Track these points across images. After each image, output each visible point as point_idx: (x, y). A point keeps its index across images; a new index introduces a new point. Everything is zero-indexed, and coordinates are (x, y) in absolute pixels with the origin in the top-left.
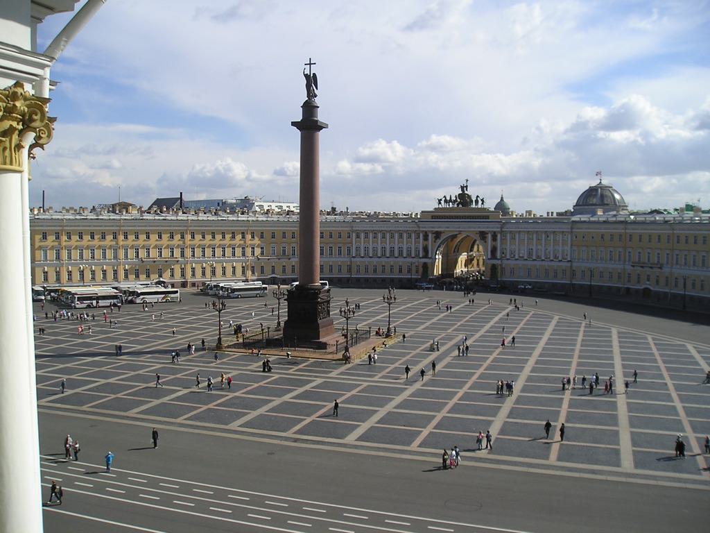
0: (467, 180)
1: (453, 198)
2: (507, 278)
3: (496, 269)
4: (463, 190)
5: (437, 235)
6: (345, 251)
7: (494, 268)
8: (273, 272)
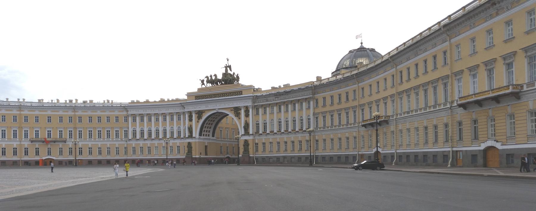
1: (214, 78)
2: (260, 154)
4: (226, 70)
5: (200, 114)
6: (122, 134)
7: (246, 143)
8: (49, 153)
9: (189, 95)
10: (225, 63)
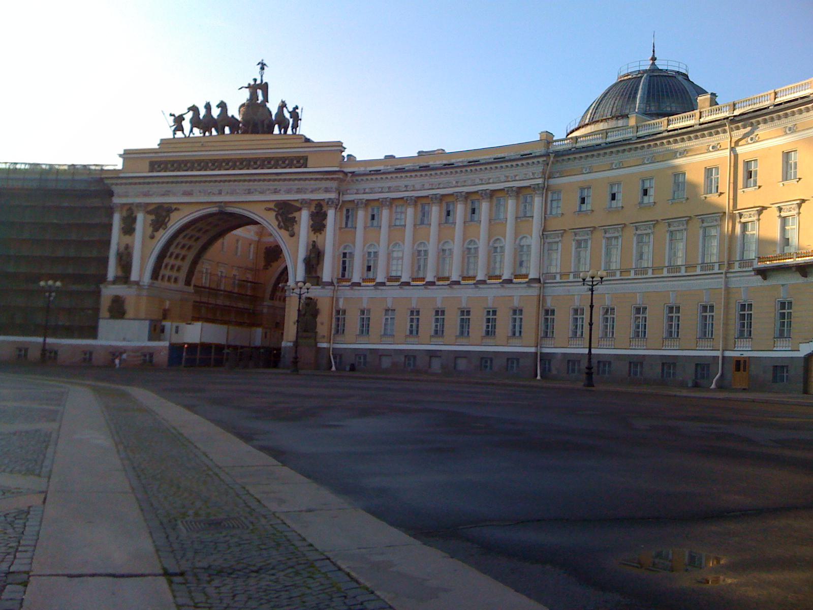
0: (263, 66)
1: (216, 112)
3: (315, 313)
4: (254, 96)
5: (160, 215)
9: (128, 156)
10: (254, 73)
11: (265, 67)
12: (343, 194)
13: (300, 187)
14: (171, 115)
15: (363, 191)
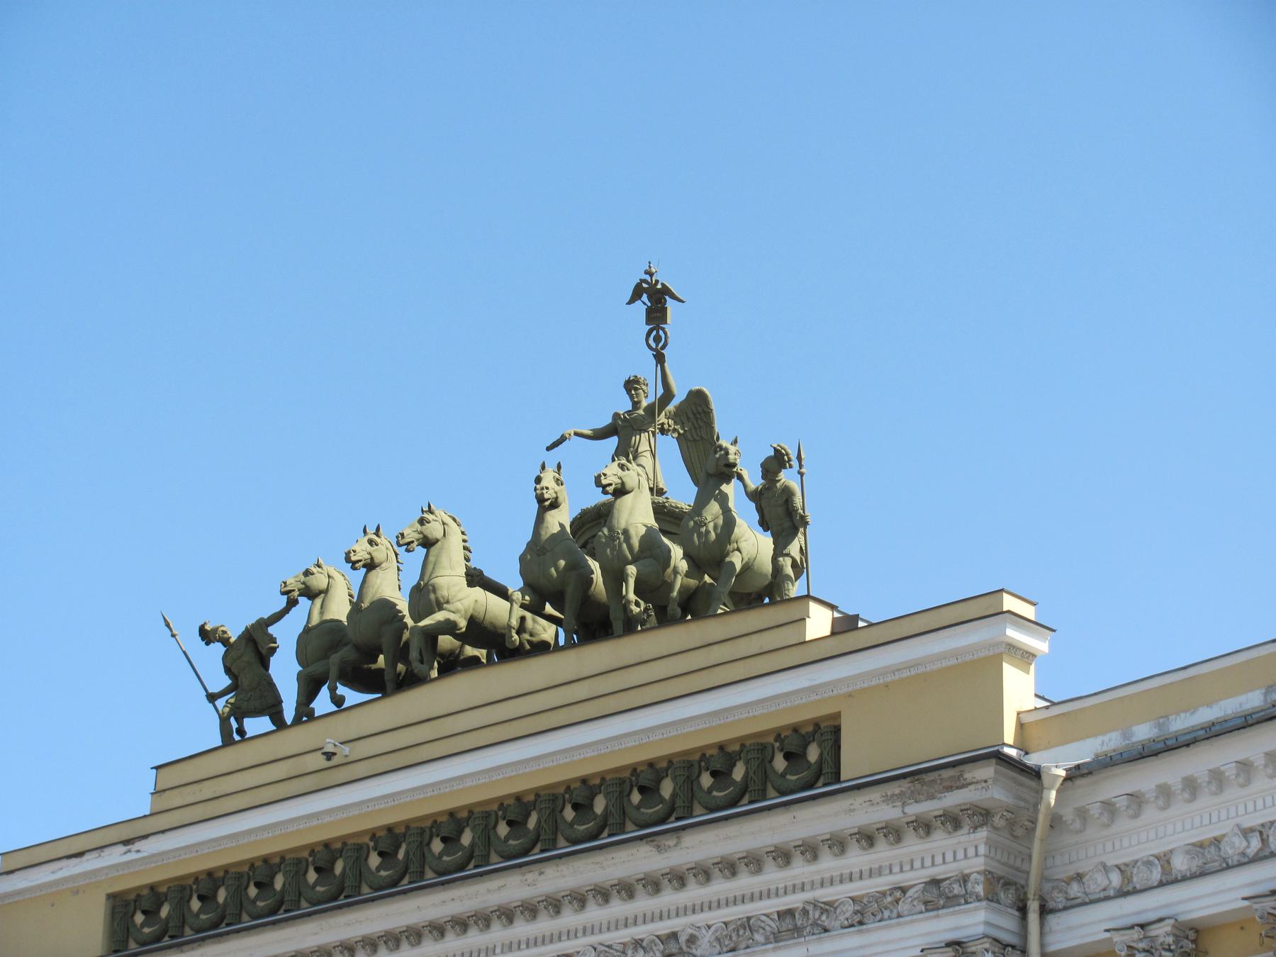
0: (655, 299)
11: (670, 303)
12: (1044, 911)
13: (795, 901)
14: (207, 636)
15: (1156, 875)
